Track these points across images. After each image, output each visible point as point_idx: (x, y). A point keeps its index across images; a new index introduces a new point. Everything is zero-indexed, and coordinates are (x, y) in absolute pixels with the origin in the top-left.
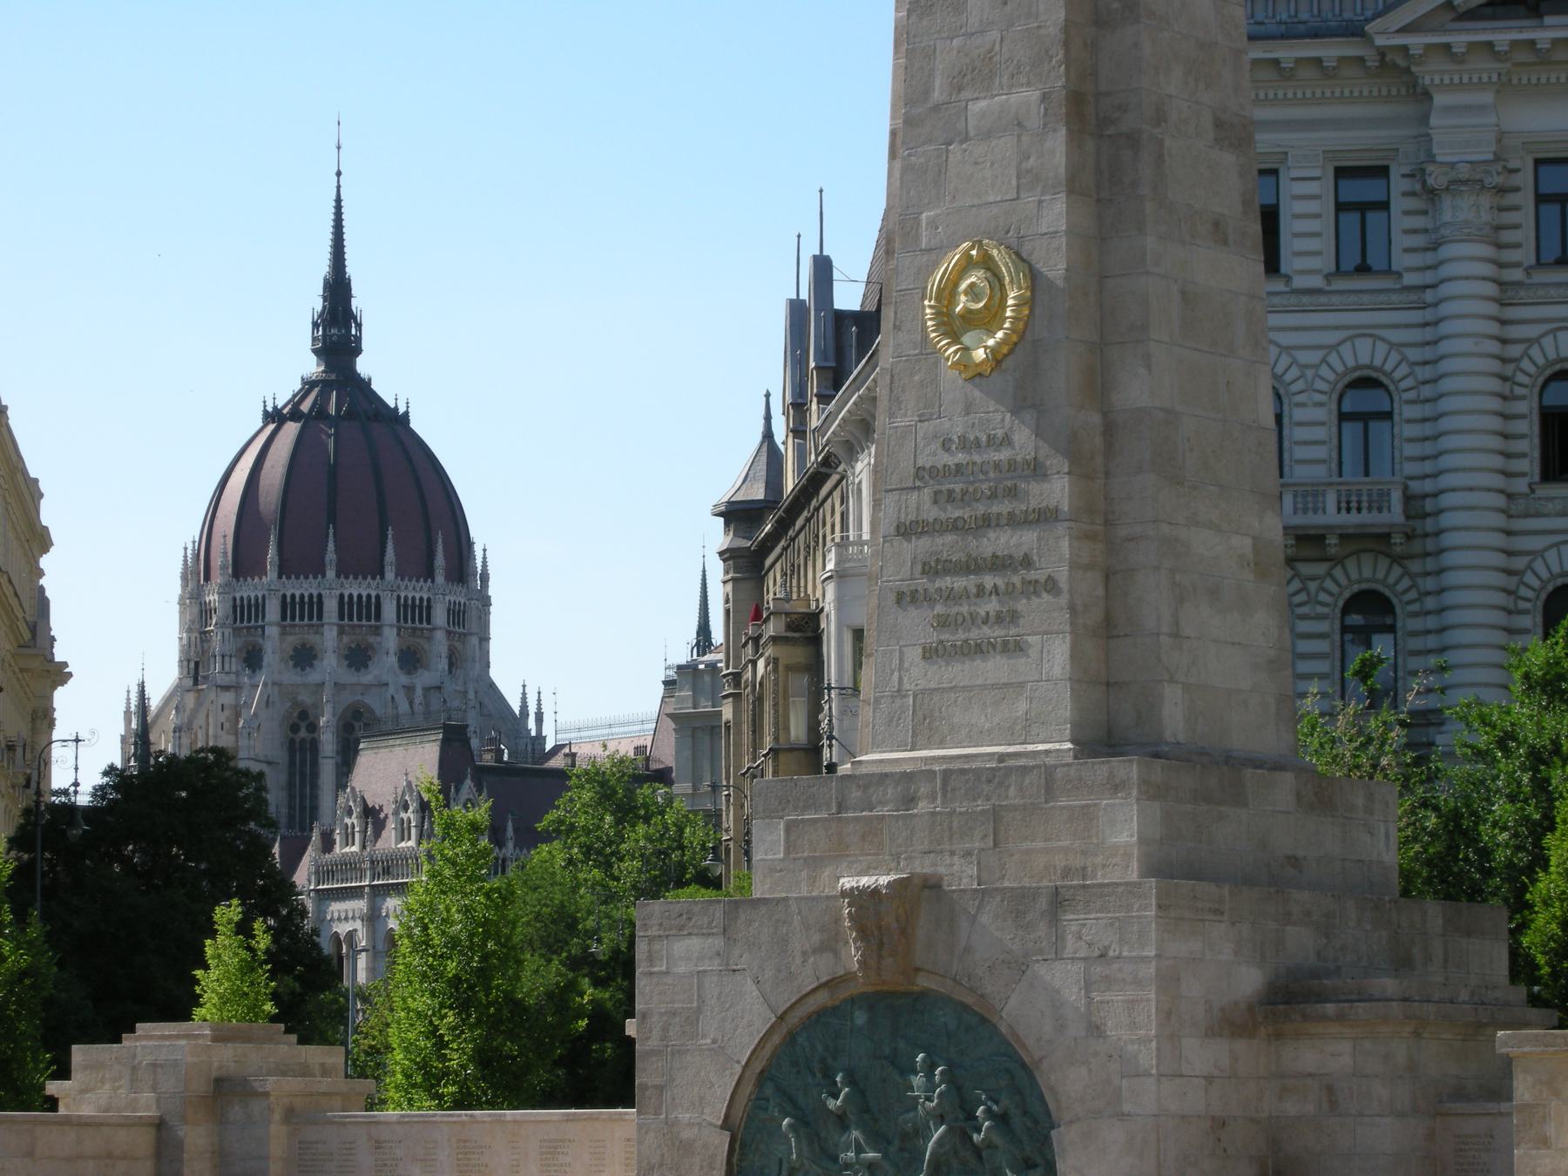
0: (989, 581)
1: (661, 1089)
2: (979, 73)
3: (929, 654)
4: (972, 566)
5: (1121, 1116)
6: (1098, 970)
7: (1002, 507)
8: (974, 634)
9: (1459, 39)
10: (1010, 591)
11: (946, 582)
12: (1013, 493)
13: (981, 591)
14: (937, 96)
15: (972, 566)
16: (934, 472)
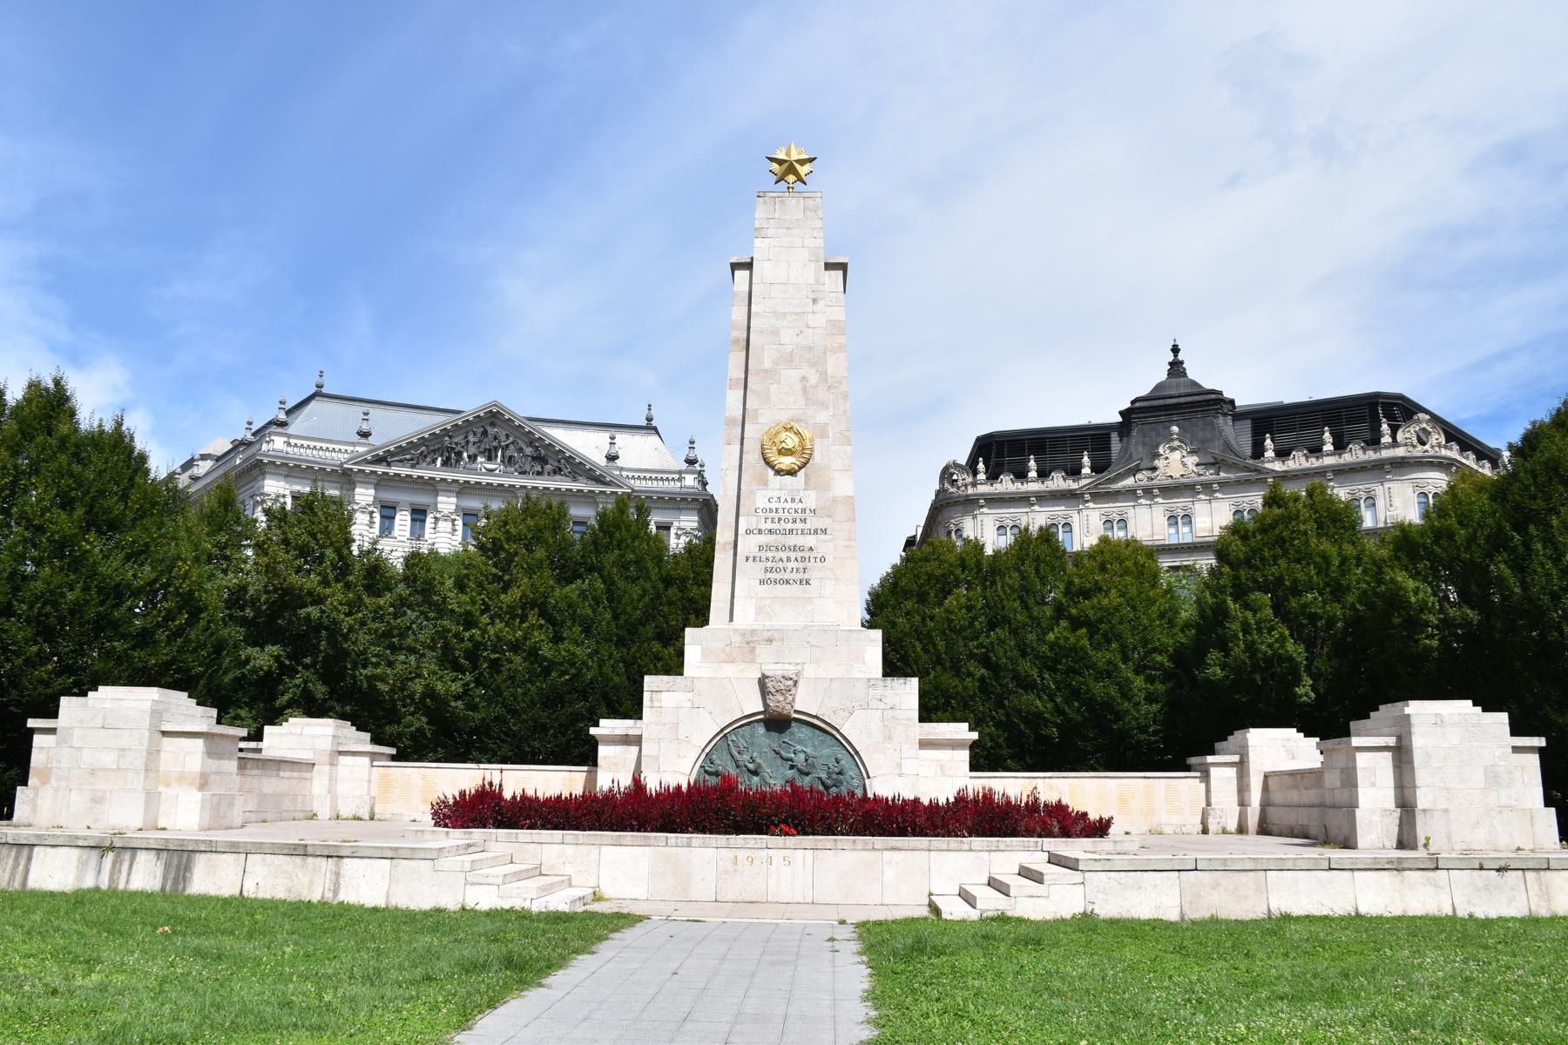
0: (793, 555)
1: (657, 758)
2: (789, 359)
3: (762, 582)
4: (785, 548)
5: (900, 775)
6: (890, 713)
7: (799, 526)
8: (786, 576)
9: (368, 469)
10: (803, 559)
11: (770, 554)
12: (804, 521)
13: (789, 559)
14: (767, 364)
15: (785, 548)
16: (765, 510)
